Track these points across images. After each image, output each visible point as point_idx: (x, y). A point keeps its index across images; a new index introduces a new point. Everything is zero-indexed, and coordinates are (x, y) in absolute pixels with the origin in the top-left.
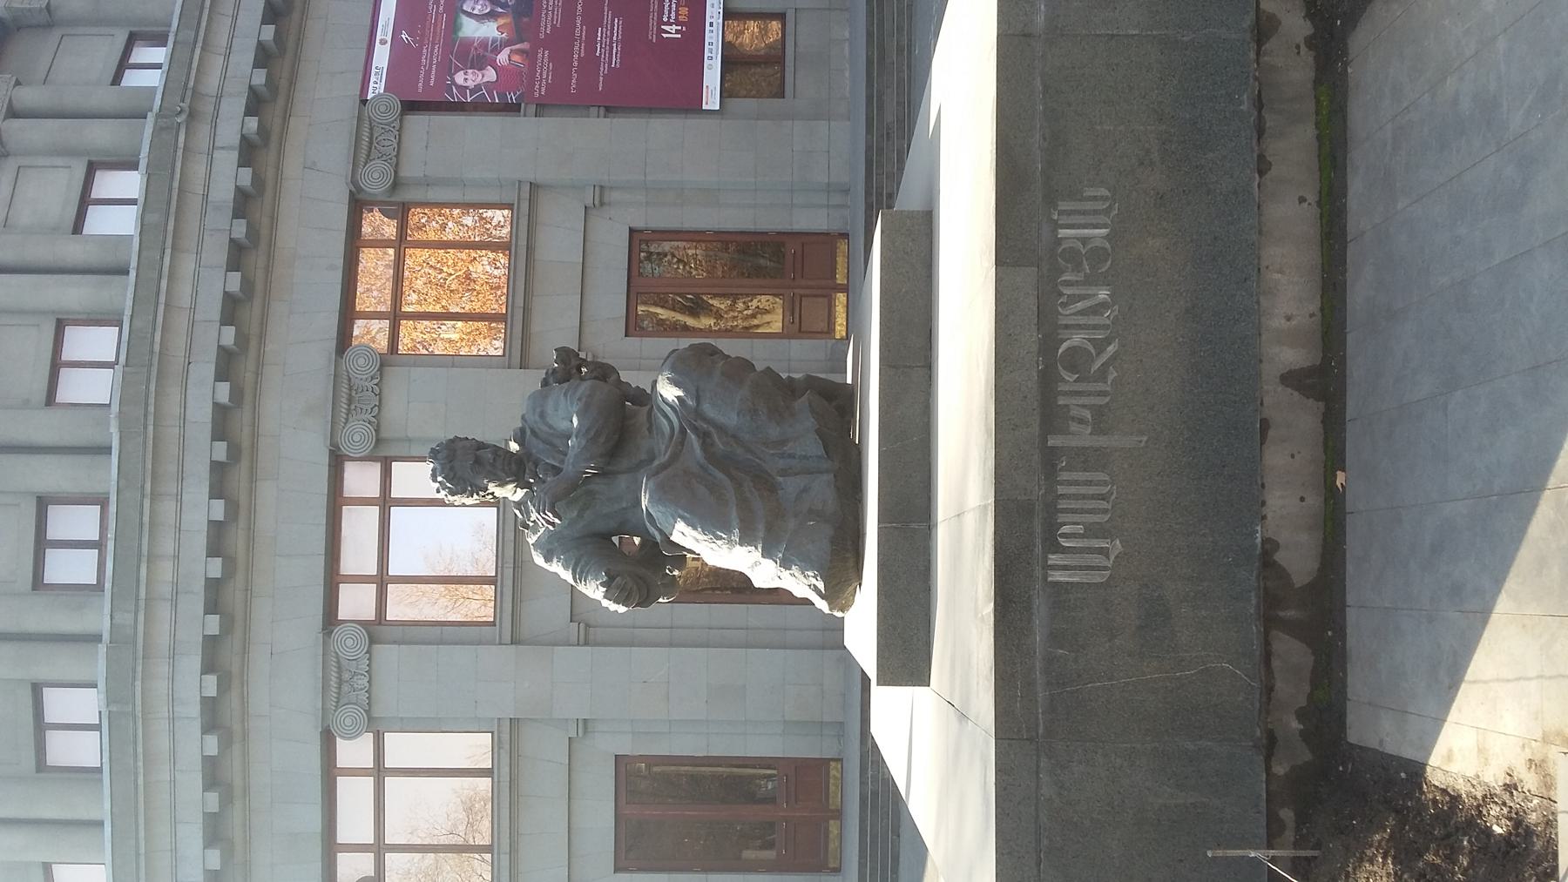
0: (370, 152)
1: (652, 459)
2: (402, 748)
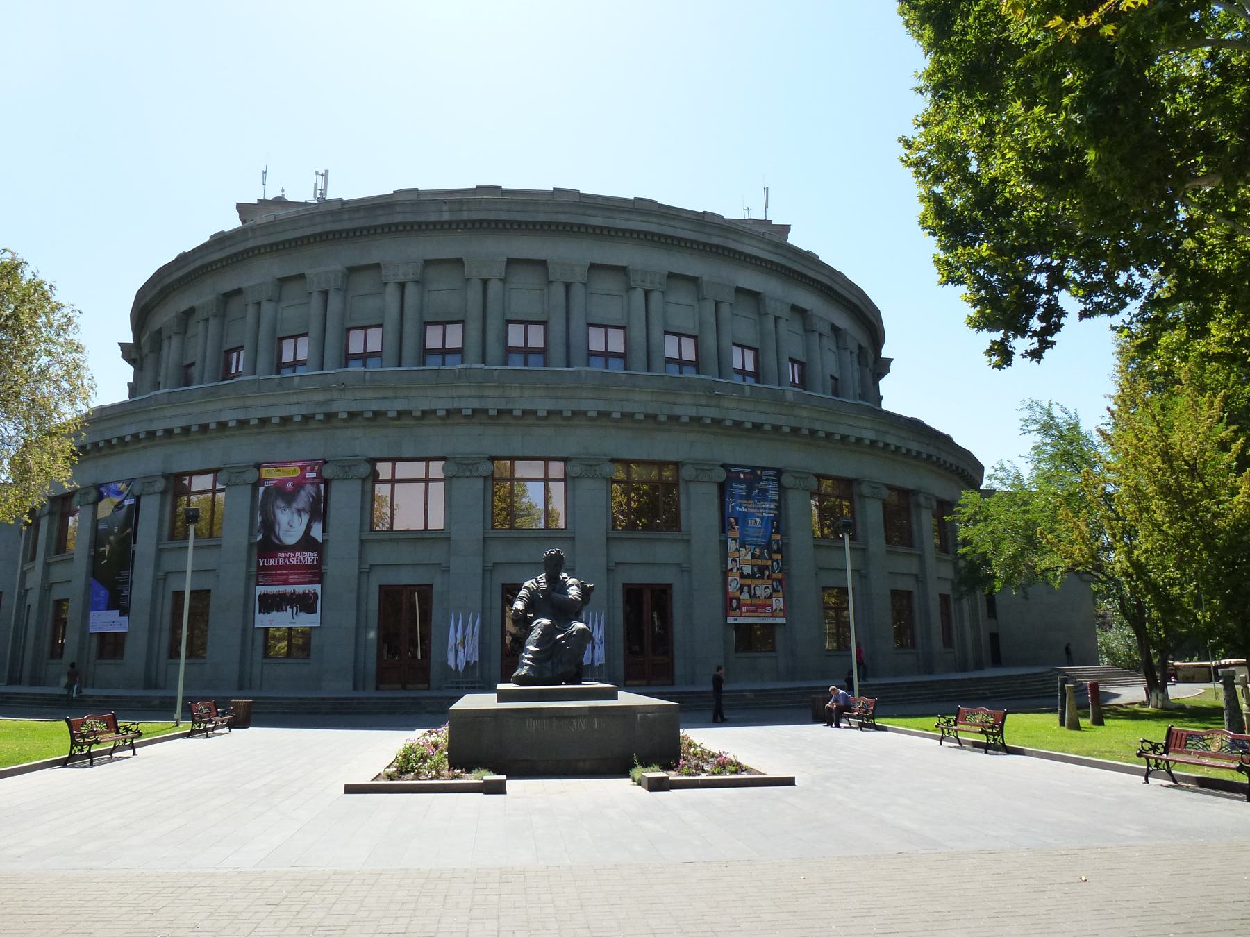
2: (437, 490)
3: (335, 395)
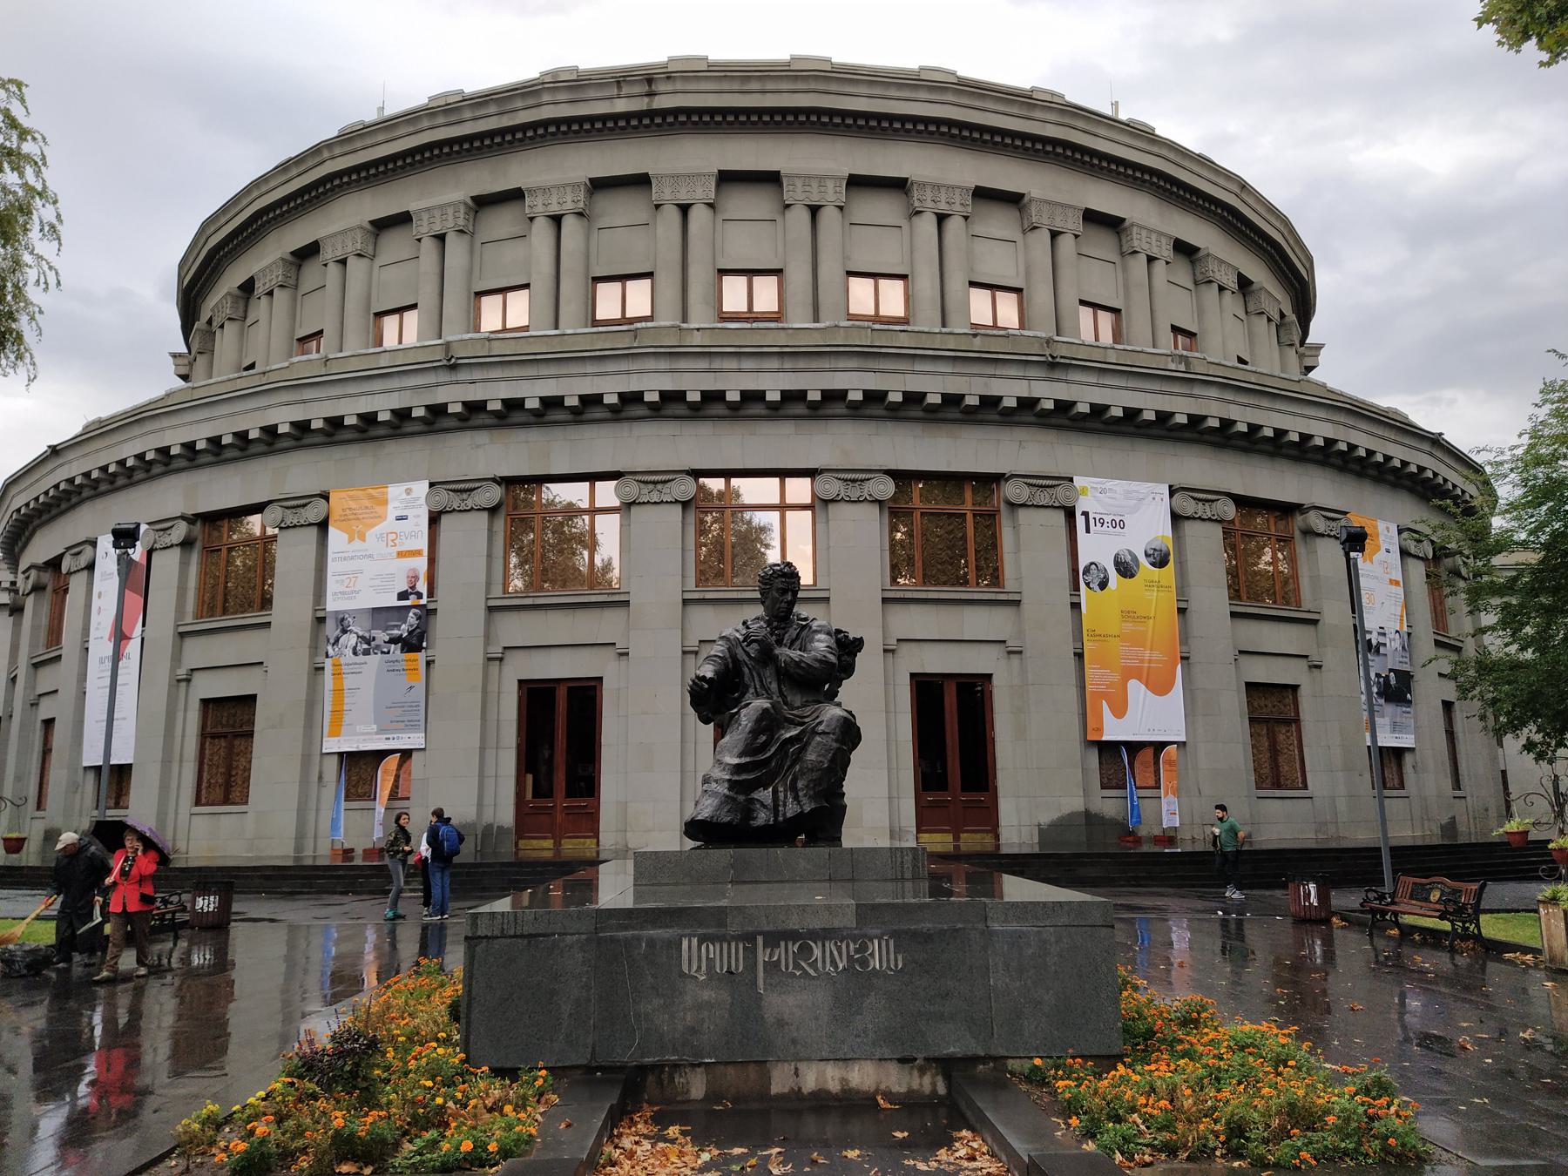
0: (1034, 485)
1: (786, 703)
3: (444, 377)
